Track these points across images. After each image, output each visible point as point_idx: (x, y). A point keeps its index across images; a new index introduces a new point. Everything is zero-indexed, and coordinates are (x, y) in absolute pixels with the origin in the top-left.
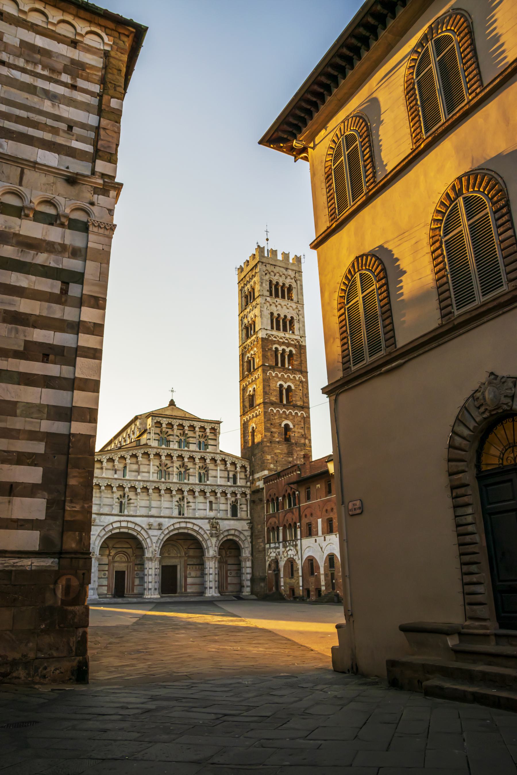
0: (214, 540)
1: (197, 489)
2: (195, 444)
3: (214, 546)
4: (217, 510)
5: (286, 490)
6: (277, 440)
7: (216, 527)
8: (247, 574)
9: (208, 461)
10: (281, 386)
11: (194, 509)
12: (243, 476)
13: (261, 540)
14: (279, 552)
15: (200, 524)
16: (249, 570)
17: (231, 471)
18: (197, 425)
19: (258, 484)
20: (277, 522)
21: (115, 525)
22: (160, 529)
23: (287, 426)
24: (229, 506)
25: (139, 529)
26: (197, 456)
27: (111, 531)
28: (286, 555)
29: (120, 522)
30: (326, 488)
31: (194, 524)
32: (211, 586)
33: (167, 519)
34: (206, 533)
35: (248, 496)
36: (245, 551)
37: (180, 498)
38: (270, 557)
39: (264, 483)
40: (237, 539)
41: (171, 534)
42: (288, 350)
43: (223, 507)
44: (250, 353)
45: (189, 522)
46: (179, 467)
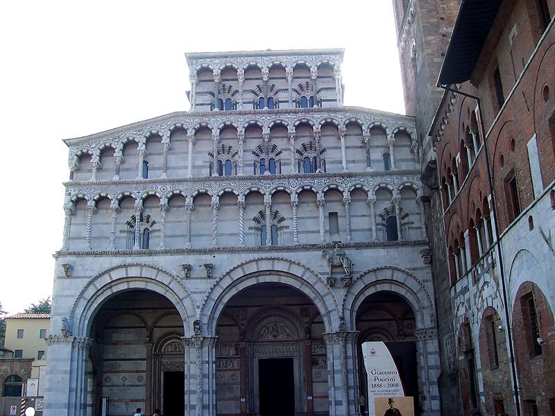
0: (340, 293)
1: (294, 188)
2: (288, 102)
3: (340, 307)
7: (342, 266)
8: (430, 368)
12: (410, 156)
14: (469, 300)
16: (433, 360)
17: (377, 147)
21: (116, 275)
22: (209, 277)
25: (166, 280)
27: (109, 285)
29: (126, 266)
30: (531, 17)
32: (339, 398)
33: (225, 256)
36: (423, 316)
37: (261, 213)
40: (402, 292)
41: (241, 287)
45: (278, 259)
46: (258, 152)
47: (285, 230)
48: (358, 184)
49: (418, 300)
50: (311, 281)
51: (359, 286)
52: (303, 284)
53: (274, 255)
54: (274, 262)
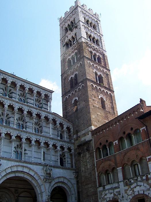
0: (47, 185)
1: (34, 138)
3: (47, 191)
4: (49, 160)
5: (124, 133)
6: (98, 106)
7: (50, 174)
9: (43, 117)
10: (96, 74)
11: (31, 157)
12: (68, 137)
13: (90, 186)
15: (35, 170)
18: (36, 90)
19: (83, 139)
20: (113, 164)
23: (102, 99)
24: (59, 158)
26: (35, 112)
28: (130, 192)
31: (30, 169)
33: (5, 161)
34: (40, 178)
35: (73, 151)
36: (72, 197)
37: (18, 145)
38: (106, 199)
39: (93, 135)
40: (66, 187)
41: (8, 177)
42: (98, 54)
43: (53, 158)
44: (71, 56)
45: (26, 167)
47: (26, 155)
48: (55, 143)
49: (70, 191)
50: (37, 178)
51: (53, 183)
52: (33, 179)
53: (25, 165)
54: (23, 168)
